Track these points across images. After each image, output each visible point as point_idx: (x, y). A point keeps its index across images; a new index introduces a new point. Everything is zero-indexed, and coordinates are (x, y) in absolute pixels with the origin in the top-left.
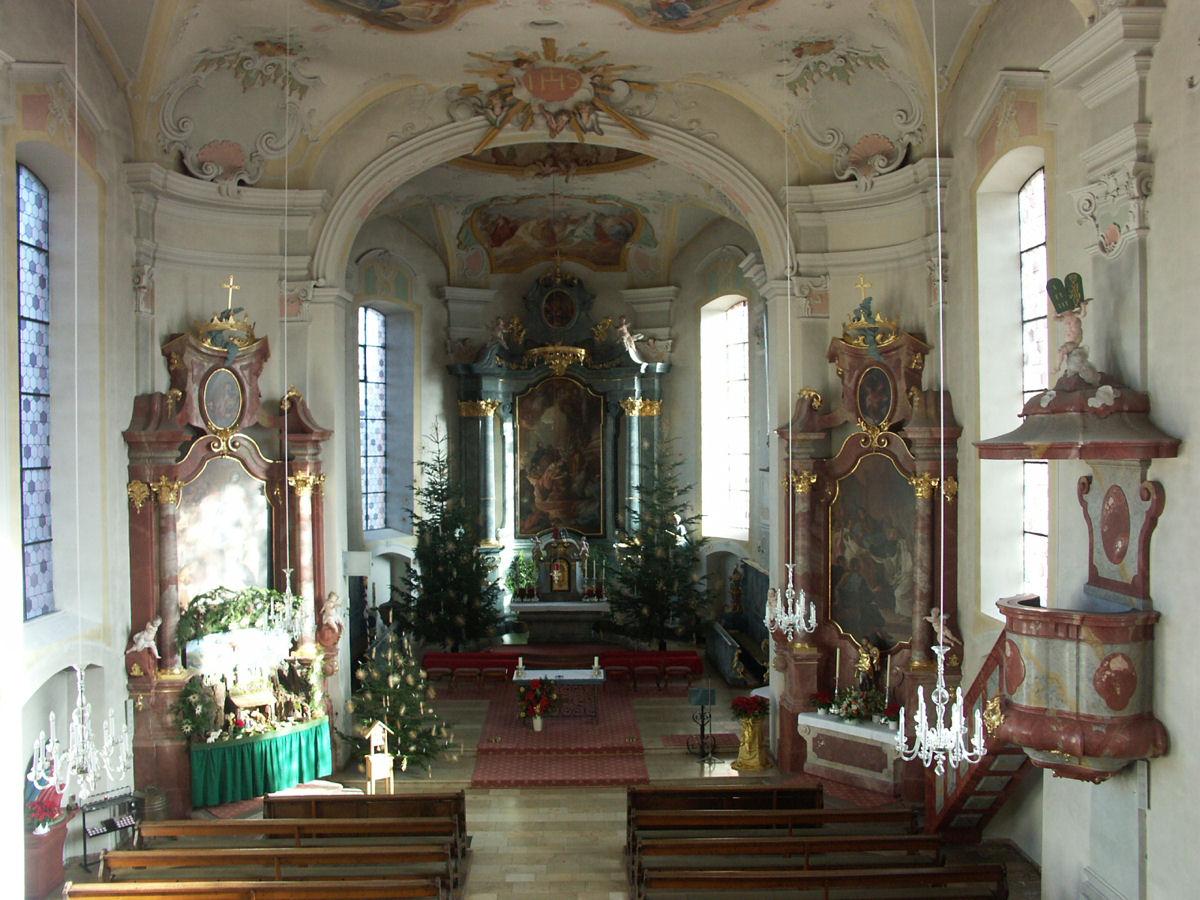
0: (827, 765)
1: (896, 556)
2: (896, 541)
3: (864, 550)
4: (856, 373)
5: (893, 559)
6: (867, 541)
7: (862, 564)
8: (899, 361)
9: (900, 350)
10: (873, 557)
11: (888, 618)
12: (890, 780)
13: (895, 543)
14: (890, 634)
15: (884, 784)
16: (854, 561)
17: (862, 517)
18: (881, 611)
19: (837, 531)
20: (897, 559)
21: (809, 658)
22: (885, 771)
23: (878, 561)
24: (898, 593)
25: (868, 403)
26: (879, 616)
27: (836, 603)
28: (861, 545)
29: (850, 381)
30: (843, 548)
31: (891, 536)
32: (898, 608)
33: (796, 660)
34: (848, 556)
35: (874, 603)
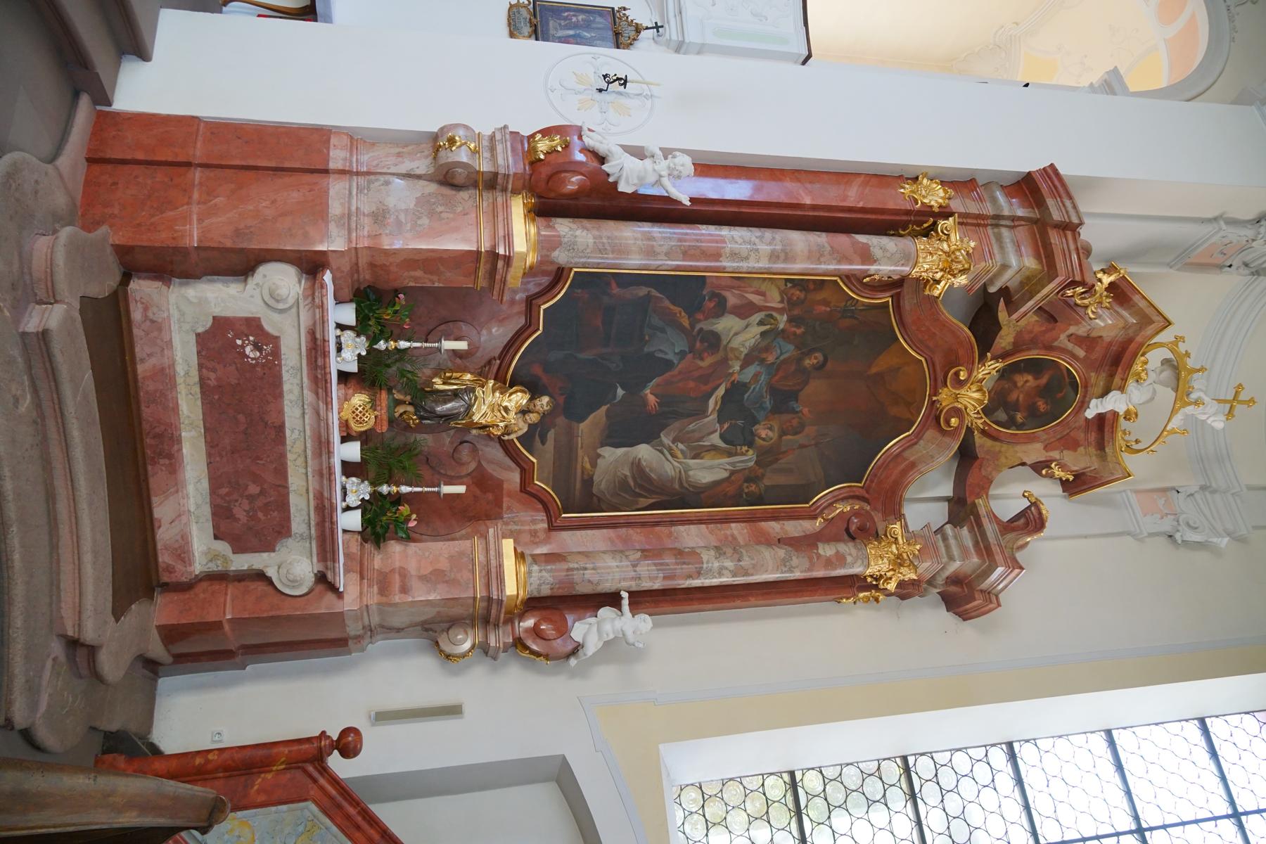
0: (180, 369)
1: (722, 445)
2: (750, 445)
3: (737, 368)
5: (715, 439)
6: (756, 375)
7: (708, 361)
9: (1092, 450)
10: (721, 391)
11: (589, 428)
12: (199, 565)
15: (183, 553)
16: (713, 341)
17: (808, 362)
18: (604, 408)
19: (782, 293)
20: (714, 448)
22: (223, 547)
23: (712, 402)
24: (644, 451)
26: (593, 408)
27: (616, 290)
28: (747, 362)
30: (744, 311)
32: (611, 455)
34: (726, 324)
35: (620, 392)
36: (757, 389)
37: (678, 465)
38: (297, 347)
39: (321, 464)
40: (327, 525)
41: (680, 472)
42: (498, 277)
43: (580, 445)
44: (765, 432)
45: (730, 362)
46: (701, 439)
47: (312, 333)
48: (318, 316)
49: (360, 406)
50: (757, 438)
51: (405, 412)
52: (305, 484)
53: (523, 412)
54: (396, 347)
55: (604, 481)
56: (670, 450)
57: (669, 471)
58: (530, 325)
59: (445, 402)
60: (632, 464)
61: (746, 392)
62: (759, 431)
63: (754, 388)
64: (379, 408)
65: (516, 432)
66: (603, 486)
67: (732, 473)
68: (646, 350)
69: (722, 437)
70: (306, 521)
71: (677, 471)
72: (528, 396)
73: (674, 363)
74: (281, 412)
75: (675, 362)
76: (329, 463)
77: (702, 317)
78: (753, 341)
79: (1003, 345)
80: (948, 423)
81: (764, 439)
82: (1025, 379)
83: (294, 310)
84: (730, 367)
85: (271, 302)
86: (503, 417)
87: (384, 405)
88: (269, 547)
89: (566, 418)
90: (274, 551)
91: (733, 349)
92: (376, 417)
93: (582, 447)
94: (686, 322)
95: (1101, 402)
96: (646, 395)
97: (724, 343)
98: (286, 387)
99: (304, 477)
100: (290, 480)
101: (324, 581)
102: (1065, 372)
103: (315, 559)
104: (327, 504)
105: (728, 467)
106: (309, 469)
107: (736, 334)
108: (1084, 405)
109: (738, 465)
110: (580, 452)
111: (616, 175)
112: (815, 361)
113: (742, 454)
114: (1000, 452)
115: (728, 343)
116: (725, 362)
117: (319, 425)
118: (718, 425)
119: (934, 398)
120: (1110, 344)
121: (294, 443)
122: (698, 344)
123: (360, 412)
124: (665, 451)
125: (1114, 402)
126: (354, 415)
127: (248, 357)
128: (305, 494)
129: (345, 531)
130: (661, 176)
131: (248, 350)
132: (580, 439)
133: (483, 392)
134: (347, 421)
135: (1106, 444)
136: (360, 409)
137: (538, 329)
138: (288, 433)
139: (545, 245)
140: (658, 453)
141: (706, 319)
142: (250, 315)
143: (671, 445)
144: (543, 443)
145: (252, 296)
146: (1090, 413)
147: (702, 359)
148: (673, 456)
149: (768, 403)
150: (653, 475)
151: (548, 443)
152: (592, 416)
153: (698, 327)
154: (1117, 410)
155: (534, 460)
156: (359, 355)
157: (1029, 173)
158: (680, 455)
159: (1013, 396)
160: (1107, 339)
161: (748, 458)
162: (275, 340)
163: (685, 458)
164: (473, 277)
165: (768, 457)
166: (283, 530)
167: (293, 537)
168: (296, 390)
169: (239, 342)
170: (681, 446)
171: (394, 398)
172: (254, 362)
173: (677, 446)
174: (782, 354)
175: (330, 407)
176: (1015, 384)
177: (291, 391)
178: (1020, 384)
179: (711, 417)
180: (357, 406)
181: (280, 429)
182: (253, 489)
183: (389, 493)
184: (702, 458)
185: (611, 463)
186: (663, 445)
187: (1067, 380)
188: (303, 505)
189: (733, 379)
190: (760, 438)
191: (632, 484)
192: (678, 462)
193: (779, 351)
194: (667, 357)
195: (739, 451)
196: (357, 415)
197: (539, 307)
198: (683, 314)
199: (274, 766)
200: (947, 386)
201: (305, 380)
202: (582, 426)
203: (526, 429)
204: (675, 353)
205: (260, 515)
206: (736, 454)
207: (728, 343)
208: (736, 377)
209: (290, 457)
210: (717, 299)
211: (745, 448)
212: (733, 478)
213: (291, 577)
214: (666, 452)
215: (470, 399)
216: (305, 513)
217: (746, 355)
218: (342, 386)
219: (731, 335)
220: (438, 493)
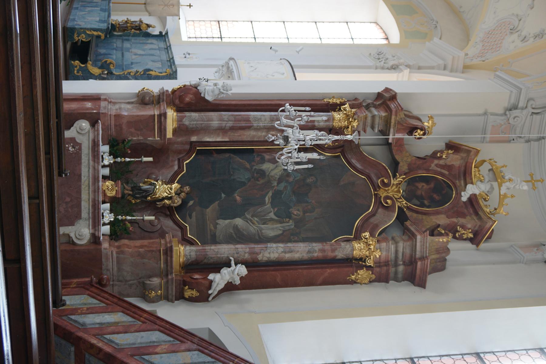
2: (290, 218)
3: (275, 184)
4: (446, 172)
5: (272, 215)
7: (262, 181)
8: (463, 216)
9: (475, 218)
10: (270, 194)
11: (210, 211)
13: (289, 216)
14: (194, 214)
16: (262, 173)
18: (217, 202)
20: (271, 220)
21: (162, 130)
23: (267, 199)
24: (238, 221)
25: (420, 185)
26: (211, 202)
27: (215, 155)
28: (280, 181)
29: (437, 165)
31: (295, 213)
32: (223, 223)
33: (160, 116)
35: (223, 195)
36: (287, 193)
37: (256, 227)
38: (88, 146)
39: (95, 187)
40: (97, 211)
41: (258, 231)
42: (163, 127)
43: (208, 219)
44: (296, 212)
45: (272, 182)
46: (265, 215)
47: (94, 141)
48: (96, 134)
50: (292, 215)
52: (88, 197)
53: (178, 194)
55: (221, 236)
56: (251, 221)
57: (252, 230)
60: (234, 227)
61: (283, 194)
62: (293, 212)
63: (286, 193)
65: (176, 203)
66: (221, 238)
67: (284, 231)
68: (232, 177)
69: (275, 214)
70: (88, 212)
71: (256, 230)
73: (246, 183)
74: (80, 170)
75: (246, 182)
76: (98, 185)
77: (255, 164)
78: (280, 173)
79: (403, 170)
80: (387, 203)
81: (296, 215)
82: (422, 185)
83: (87, 135)
84: (272, 184)
85: (80, 131)
87: (119, 186)
88: (72, 224)
90: (74, 225)
91: (272, 176)
92: (116, 190)
93: (209, 220)
94: (248, 166)
95: (466, 192)
96: (235, 197)
97: (267, 174)
98: (83, 161)
99: (88, 194)
100: (82, 196)
101: (95, 239)
102: (442, 182)
103: (91, 227)
104: (97, 202)
105: (281, 228)
106: (90, 190)
107: (272, 170)
108: (459, 195)
109: (286, 227)
110: (208, 222)
111: (204, 92)
112: (312, 180)
113: (288, 222)
114: (422, 219)
115: (269, 174)
116: (269, 182)
117: (95, 173)
118: (272, 209)
119: (376, 192)
120: (459, 167)
121: (85, 181)
122: (255, 175)
124: (249, 221)
125: (471, 190)
127: (70, 151)
128: (88, 202)
129: (103, 235)
130: (220, 89)
131: (70, 148)
134: (104, 191)
135: (478, 210)
138: (83, 177)
139: (180, 120)
140: (246, 222)
141: (257, 165)
142: (72, 137)
143: (251, 218)
144: (191, 218)
145: (73, 131)
146: (465, 198)
147: (258, 181)
148: (253, 223)
149: (294, 199)
150: (245, 233)
152: (211, 206)
153: (254, 167)
154: (475, 193)
155: (187, 225)
157: (379, 93)
158: (256, 223)
159: (419, 193)
160: (457, 166)
161: (290, 224)
162: (80, 145)
163: (259, 224)
164: (153, 131)
165: (299, 223)
166: (78, 216)
167: (82, 219)
168: (87, 162)
169: (67, 146)
170: (255, 219)
172: (72, 152)
173: (254, 219)
174: (295, 177)
175: (99, 164)
176: (417, 187)
177: (85, 162)
178: (420, 187)
179: (268, 206)
181: (80, 176)
182: (68, 199)
183: (121, 161)
184: (267, 224)
185: (224, 227)
186: (248, 219)
187: (445, 185)
188: (87, 206)
189: (275, 188)
190: (294, 214)
191: (235, 237)
192: (256, 226)
193: (294, 177)
194: (242, 180)
195: (285, 221)
197: (184, 162)
198: (246, 163)
199: (71, 285)
200: (381, 188)
201: (90, 156)
202: (208, 210)
203: (180, 202)
204: (246, 179)
205: (70, 210)
206: (284, 222)
207: (269, 174)
208: (275, 188)
209: (83, 187)
210: (260, 157)
211: (287, 220)
212: (285, 234)
213: (80, 234)
214: (249, 221)
216: (87, 209)
217: (279, 179)
218: (103, 180)
219: (270, 170)
220: (143, 219)
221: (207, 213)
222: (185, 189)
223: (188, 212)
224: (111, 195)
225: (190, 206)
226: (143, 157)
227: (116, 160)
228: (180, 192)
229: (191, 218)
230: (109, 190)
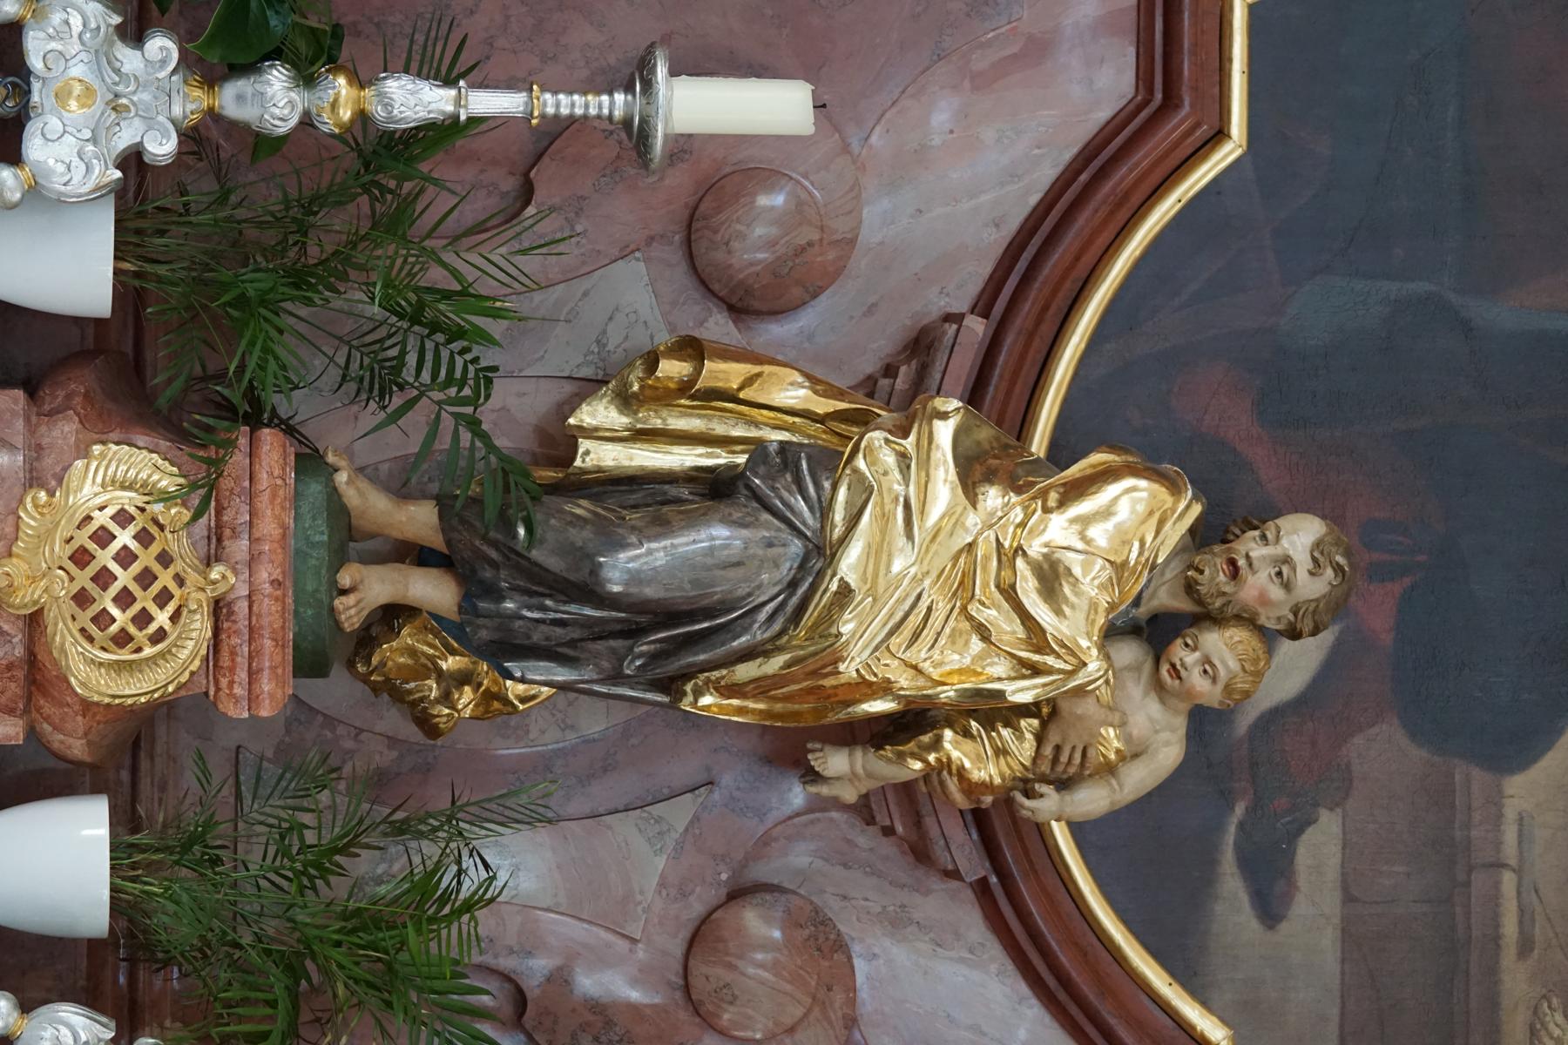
43: (1510, 928)
49: (123, 518)
51: (393, 615)
54: (362, 117)
58: (1171, 101)
59: (661, 526)
64: (239, 548)
65: (1109, 770)
72: (1188, 510)
86: (1035, 634)
87: (268, 527)
89: (1414, 735)
92: (220, 609)
93: (1526, 946)
123: (125, 557)
126: (84, 578)
132: (1508, 880)
133: (903, 456)
134: (34, 621)
136: (125, 538)
137: (1220, 135)
144: (1270, 909)
151: (1301, 908)
156: (133, 161)
171: (333, 494)
180: (102, 519)
196: (104, 578)
203: (1168, 753)
215: (824, 510)
221: (1510, 835)
222: (1258, 584)
223: (1240, 810)
224: (137, 688)
225: (1275, 715)
226: (661, 71)
227: (235, 100)
228: (1184, 605)
229: (1270, 909)
230: (103, 619)
